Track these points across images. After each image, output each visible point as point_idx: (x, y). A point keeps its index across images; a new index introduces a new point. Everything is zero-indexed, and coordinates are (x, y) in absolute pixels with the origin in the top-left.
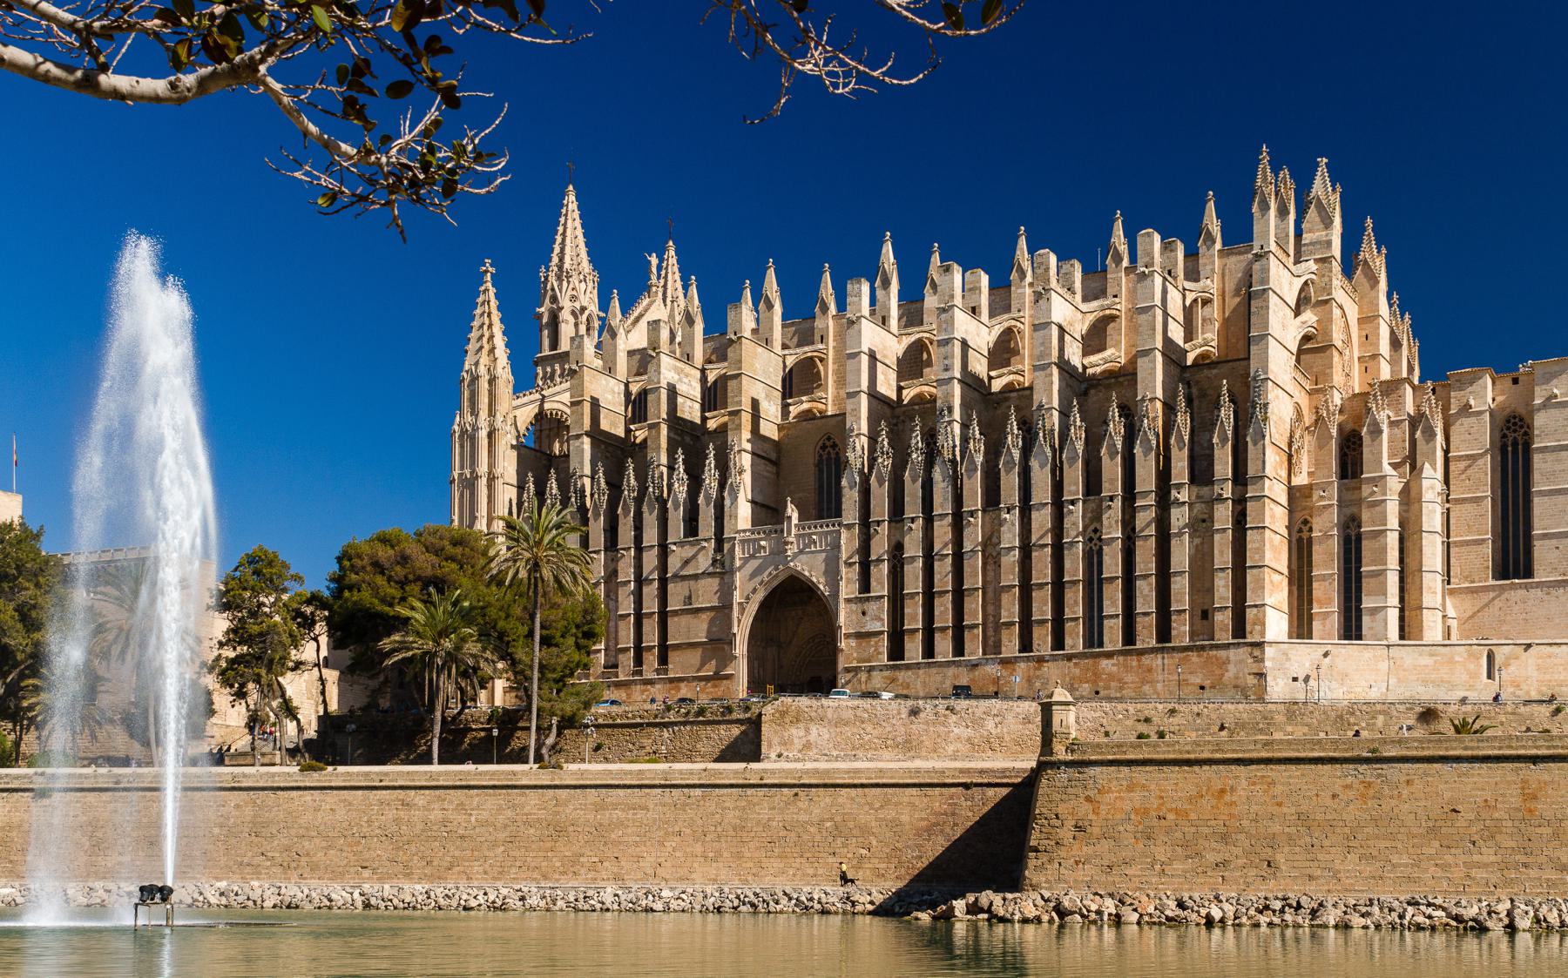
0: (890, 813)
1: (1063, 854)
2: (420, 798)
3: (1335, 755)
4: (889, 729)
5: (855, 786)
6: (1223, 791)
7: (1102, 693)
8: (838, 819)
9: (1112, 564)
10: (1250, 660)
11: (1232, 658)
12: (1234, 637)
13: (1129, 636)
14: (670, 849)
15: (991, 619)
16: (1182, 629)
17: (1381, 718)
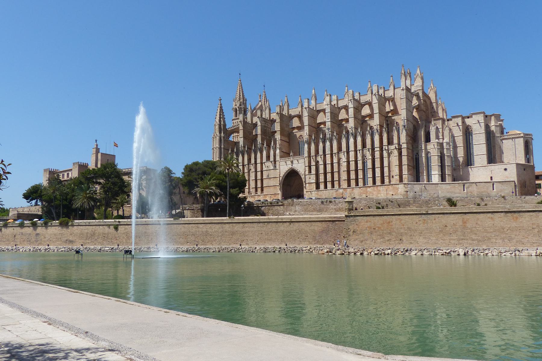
0: (312, 228)
1: (351, 238)
2: (201, 226)
3: (417, 213)
4: (315, 207)
6: (389, 222)
7: (368, 196)
9: (369, 164)
10: (405, 188)
11: (400, 187)
13: (374, 182)
16: (386, 180)
17: (437, 201)
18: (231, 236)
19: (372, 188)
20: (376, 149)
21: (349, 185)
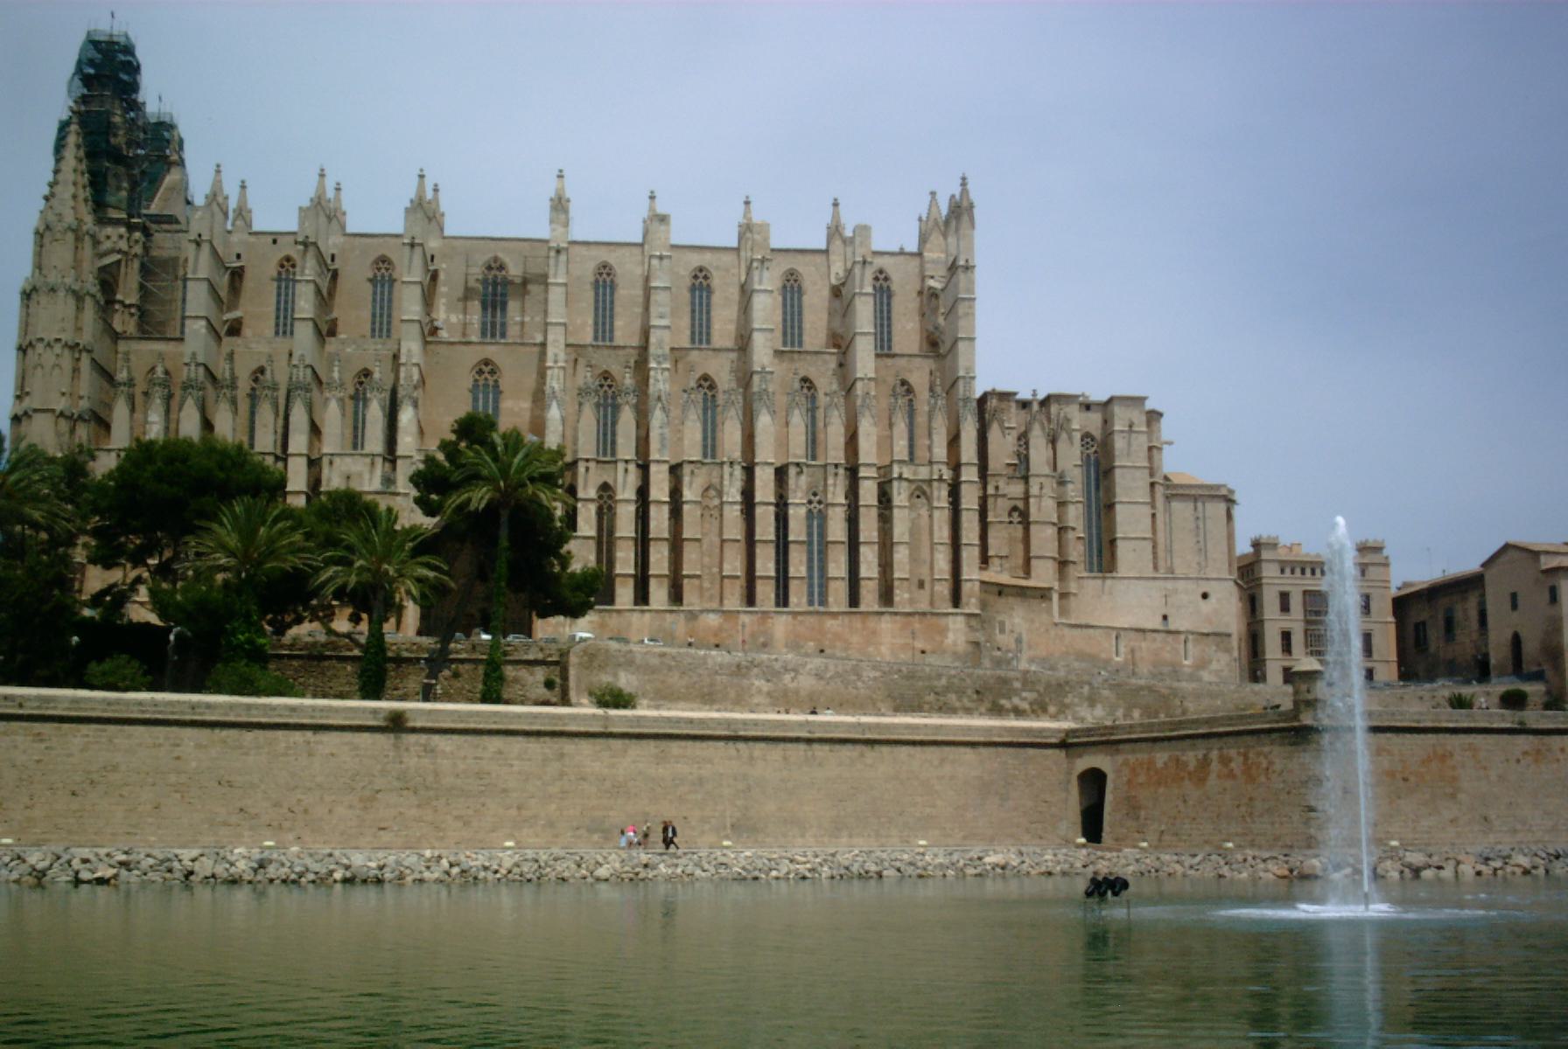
4: (695, 679)
7: (828, 651)
9: (837, 529)
11: (951, 626)
13: (854, 600)
16: (901, 595)
19: (846, 619)
20: (863, 473)
21: (750, 599)
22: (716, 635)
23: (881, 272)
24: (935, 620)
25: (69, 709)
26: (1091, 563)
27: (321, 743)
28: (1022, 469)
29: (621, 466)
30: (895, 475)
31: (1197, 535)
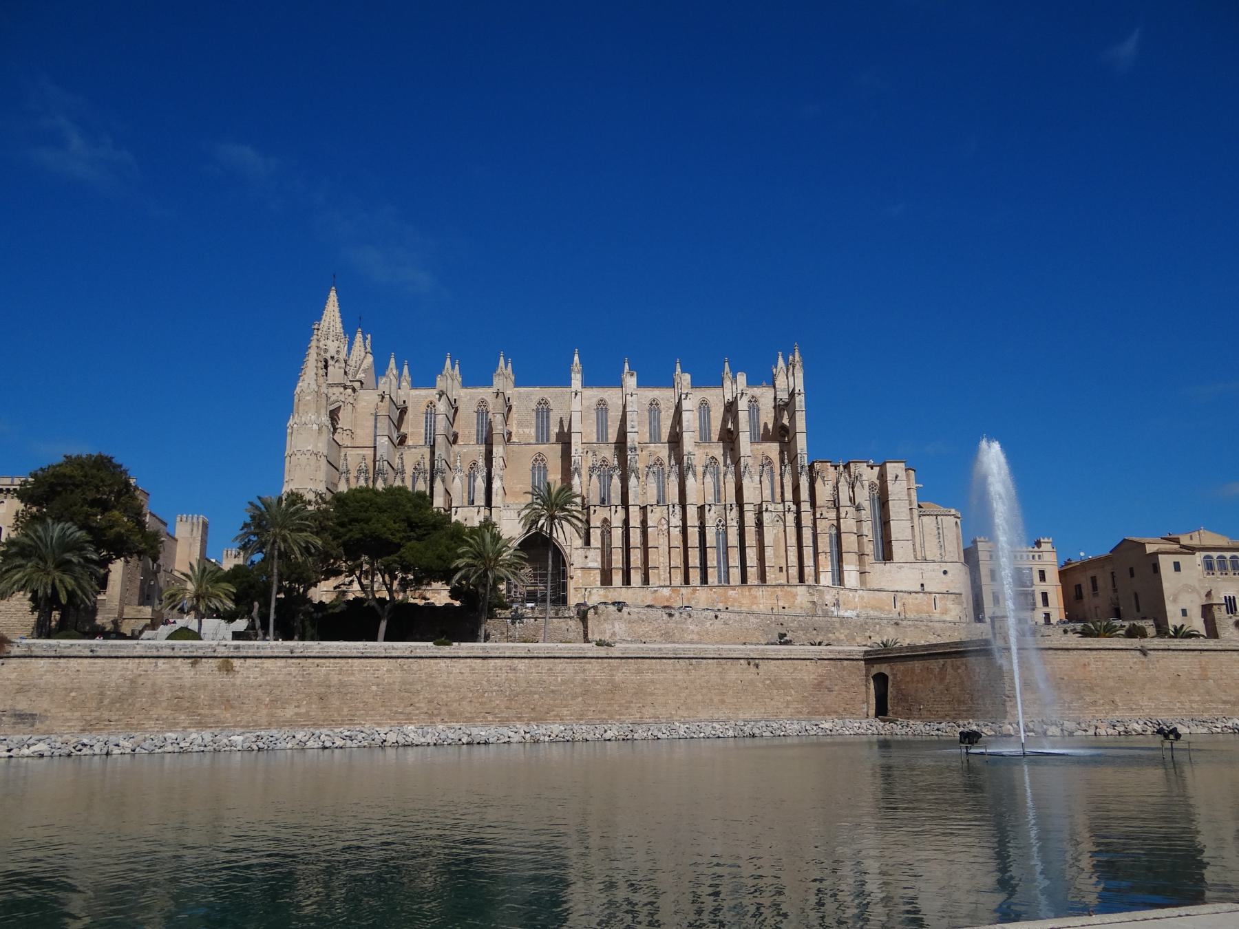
2: (521, 665)
4: (657, 626)
5: (778, 659)
6: (1085, 665)
8: (772, 678)
9: (733, 539)
12: (800, 582)
13: (744, 579)
14: (683, 698)
15: (662, 565)
16: (771, 576)
18: (610, 696)
20: (746, 507)
22: (668, 600)
23: (753, 397)
24: (789, 589)
25: (319, 652)
26: (878, 556)
27: (454, 666)
28: (836, 505)
29: (613, 508)
30: (764, 509)
31: (939, 538)
